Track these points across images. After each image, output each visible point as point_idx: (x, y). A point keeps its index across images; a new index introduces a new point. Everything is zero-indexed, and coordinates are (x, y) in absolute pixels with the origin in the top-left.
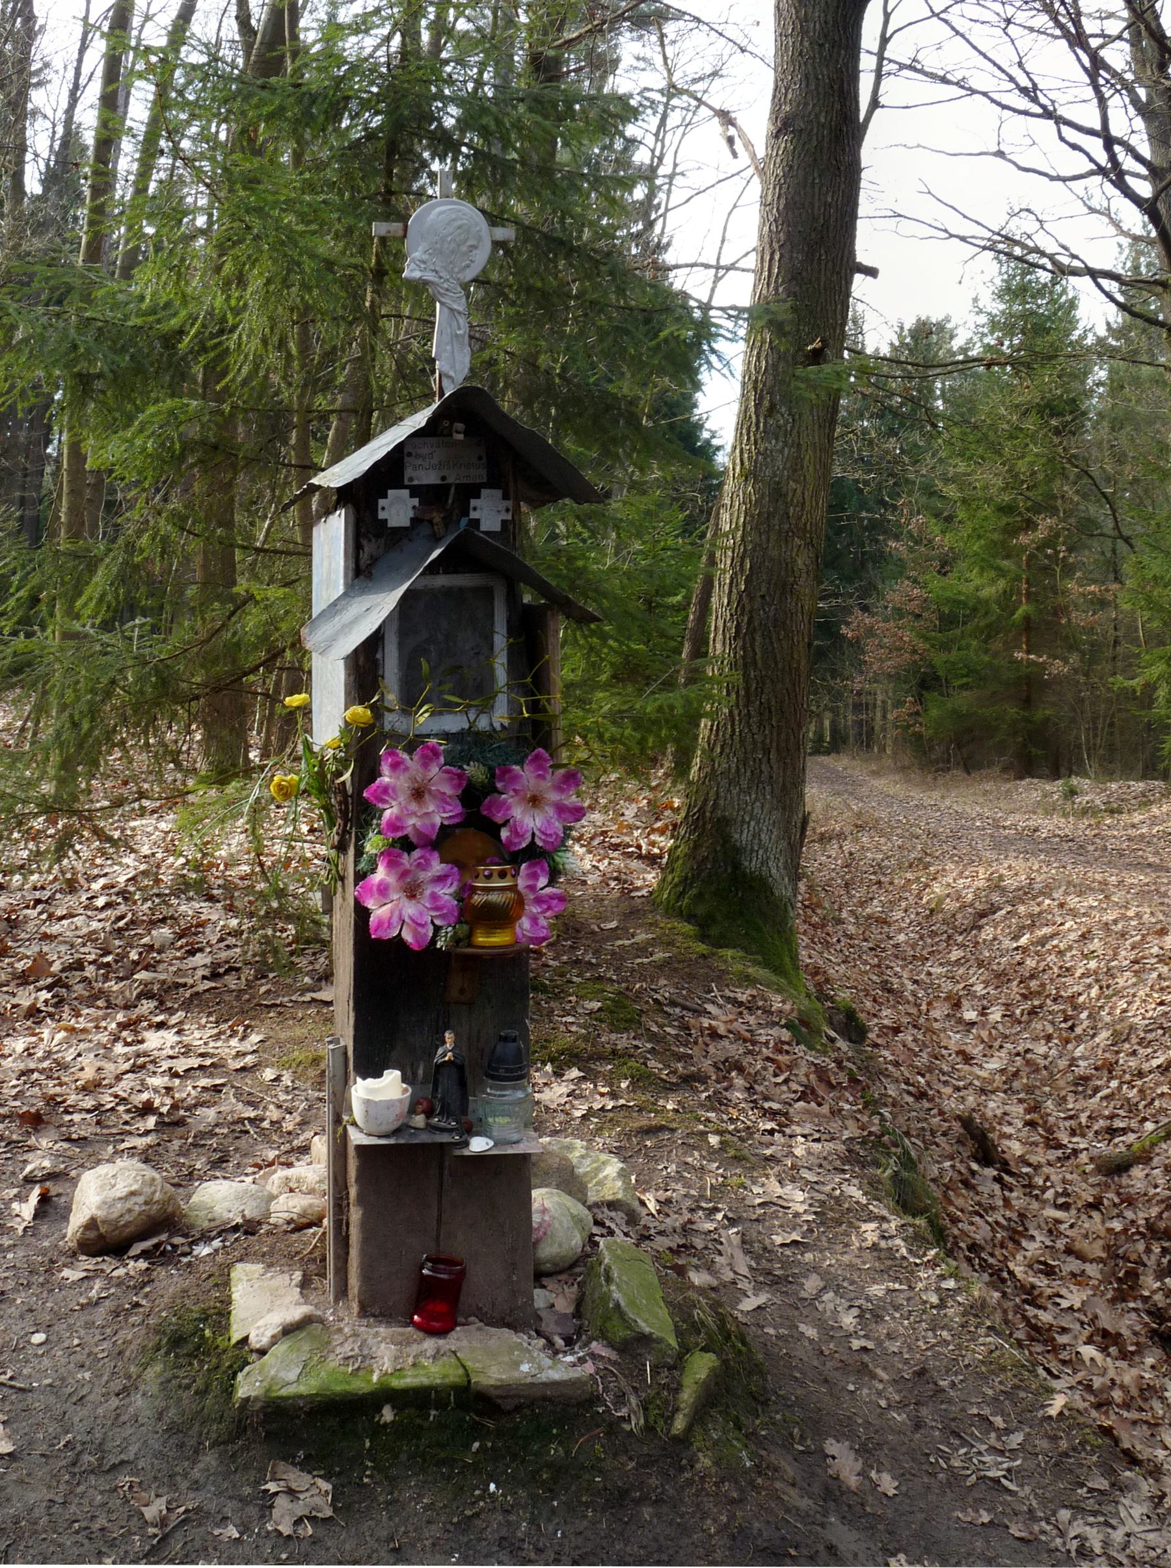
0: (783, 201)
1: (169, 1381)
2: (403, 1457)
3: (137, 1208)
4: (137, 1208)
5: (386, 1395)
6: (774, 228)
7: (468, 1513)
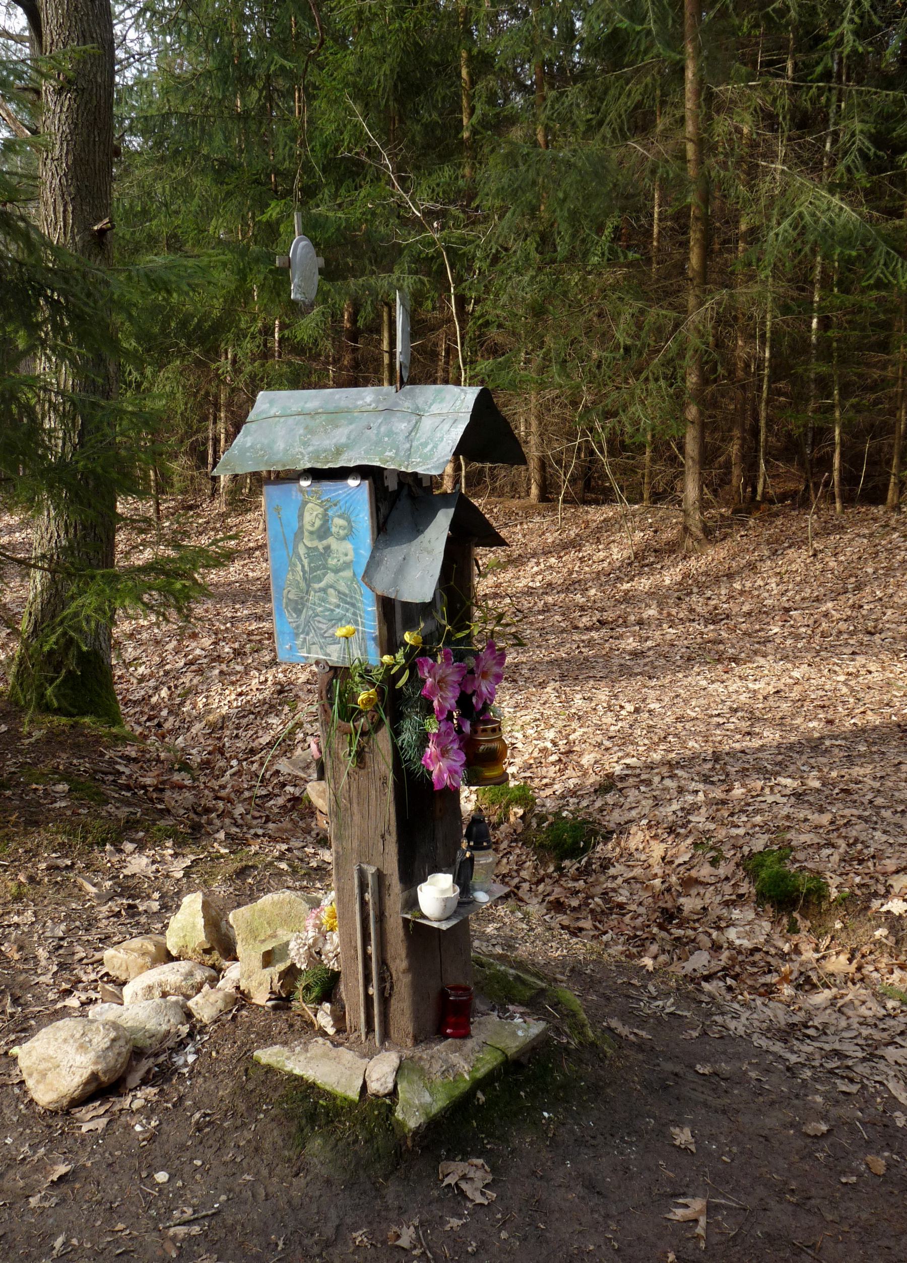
0: (71, 157)
1: (336, 1145)
2: (497, 1121)
3: (124, 1050)
4: (124, 1050)
5: (479, 1084)
6: (64, 181)
7: (550, 1135)
